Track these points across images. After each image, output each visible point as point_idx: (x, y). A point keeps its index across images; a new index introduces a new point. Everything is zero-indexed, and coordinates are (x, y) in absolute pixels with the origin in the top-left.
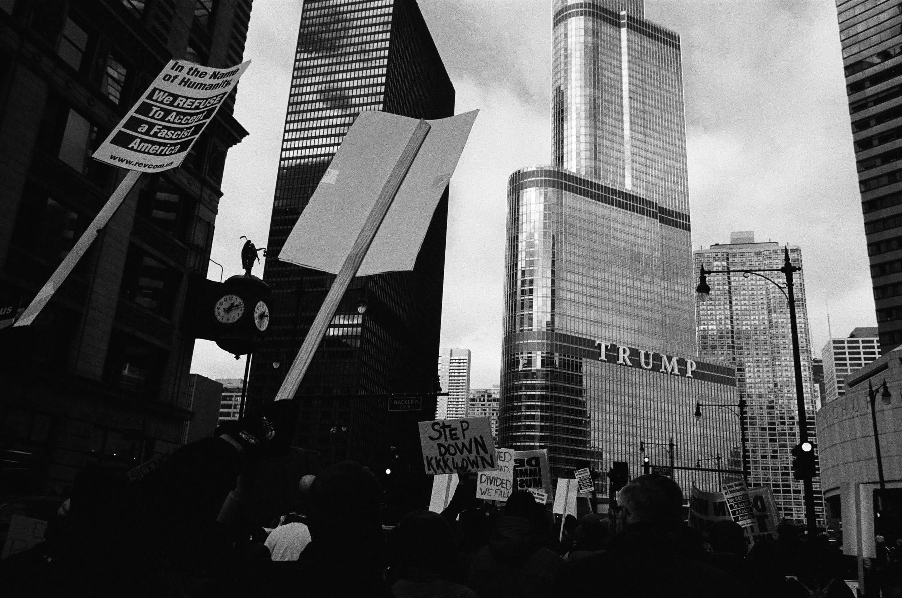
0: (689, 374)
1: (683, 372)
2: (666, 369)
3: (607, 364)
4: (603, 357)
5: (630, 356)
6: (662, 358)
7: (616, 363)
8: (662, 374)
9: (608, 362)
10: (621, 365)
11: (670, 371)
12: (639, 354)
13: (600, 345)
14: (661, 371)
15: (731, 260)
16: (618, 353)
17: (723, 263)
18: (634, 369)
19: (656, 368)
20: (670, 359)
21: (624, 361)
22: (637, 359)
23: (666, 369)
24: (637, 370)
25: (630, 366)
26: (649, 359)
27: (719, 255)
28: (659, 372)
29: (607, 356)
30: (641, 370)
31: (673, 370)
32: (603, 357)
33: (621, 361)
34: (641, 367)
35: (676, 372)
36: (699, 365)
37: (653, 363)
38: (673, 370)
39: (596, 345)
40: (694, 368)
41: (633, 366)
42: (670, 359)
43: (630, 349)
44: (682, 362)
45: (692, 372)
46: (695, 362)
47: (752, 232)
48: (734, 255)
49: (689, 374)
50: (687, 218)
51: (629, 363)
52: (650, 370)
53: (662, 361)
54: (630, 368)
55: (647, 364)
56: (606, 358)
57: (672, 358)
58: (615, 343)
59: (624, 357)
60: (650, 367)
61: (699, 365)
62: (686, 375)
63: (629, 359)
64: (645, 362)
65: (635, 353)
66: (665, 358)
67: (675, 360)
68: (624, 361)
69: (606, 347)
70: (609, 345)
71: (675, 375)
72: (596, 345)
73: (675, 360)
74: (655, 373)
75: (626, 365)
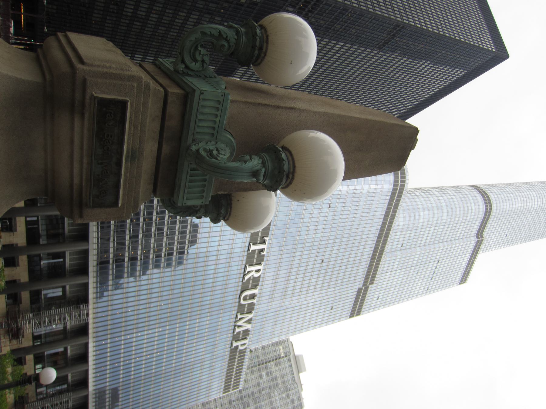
0: (235, 344)
1: (236, 338)
2: (240, 319)
3: (246, 253)
4: (253, 248)
5: (254, 278)
6: (251, 312)
7: (246, 263)
8: (235, 316)
9: (248, 254)
10: (245, 269)
11: (239, 323)
12: (255, 287)
13: (264, 242)
14: (239, 314)
15: (285, 359)
16: (256, 264)
17: (283, 354)
18: (240, 284)
19: (241, 309)
20: (249, 321)
21: (249, 272)
22: (250, 286)
23: (240, 319)
24: (240, 288)
25: (243, 279)
26: (250, 299)
27: (288, 350)
28: (237, 313)
29: (254, 251)
30: (239, 292)
31: (239, 326)
32: (253, 248)
33: (249, 269)
34: (242, 292)
35: (237, 330)
36: (243, 352)
37: (245, 305)
38: (239, 326)
39: (265, 238)
40: (241, 348)
41: (243, 283)
42: (249, 321)
43: (259, 277)
44: (246, 333)
45: (237, 347)
46: (246, 349)
47: (305, 370)
48: (289, 360)
49: (235, 344)
50: (359, 314)
51: (247, 278)
52: (239, 302)
53: (247, 313)
54: (241, 279)
55: (245, 299)
56: (252, 251)
57: (250, 323)
58: (265, 259)
59: (253, 271)
60: (242, 302)
61: (243, 352)
62: (234, 342)
63: (249, 279)
64: (246, 296)
65: (256, 282)
66: (250, 316)
67: (249, 326)
68: (249, 272)
69: (262, 250)
70: (265, 253)
71: (234, 330)
72: (265, 238)
73: (249, 326)
74: (236, 308)
75: (245, 275)
